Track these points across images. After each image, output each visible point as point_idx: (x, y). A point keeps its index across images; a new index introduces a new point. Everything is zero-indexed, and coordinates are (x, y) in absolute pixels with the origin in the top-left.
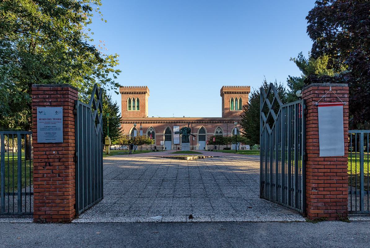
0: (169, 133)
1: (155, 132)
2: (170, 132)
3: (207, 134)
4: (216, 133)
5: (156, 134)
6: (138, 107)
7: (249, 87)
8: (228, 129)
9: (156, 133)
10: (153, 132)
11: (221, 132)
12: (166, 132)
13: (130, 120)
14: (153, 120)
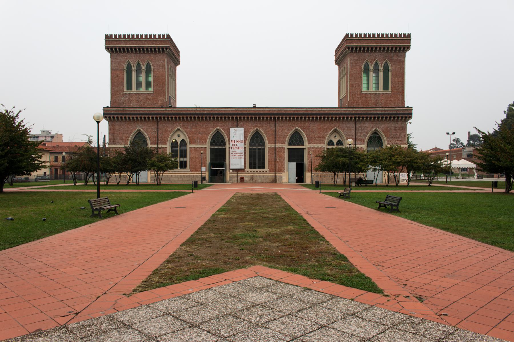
0: (220, 145)
1: (188, 141)
2: (223, 142)
3: (306, 145)
4: (329, 144)
5: (189, 146)
6: (148, 84)
7: (409, 35)
8: (358, 134)
9: (191, 143)
10: (183, 141)
11: (339, 143)
12: (214, 141)
13: (129, 112)
14: (184, 112)
